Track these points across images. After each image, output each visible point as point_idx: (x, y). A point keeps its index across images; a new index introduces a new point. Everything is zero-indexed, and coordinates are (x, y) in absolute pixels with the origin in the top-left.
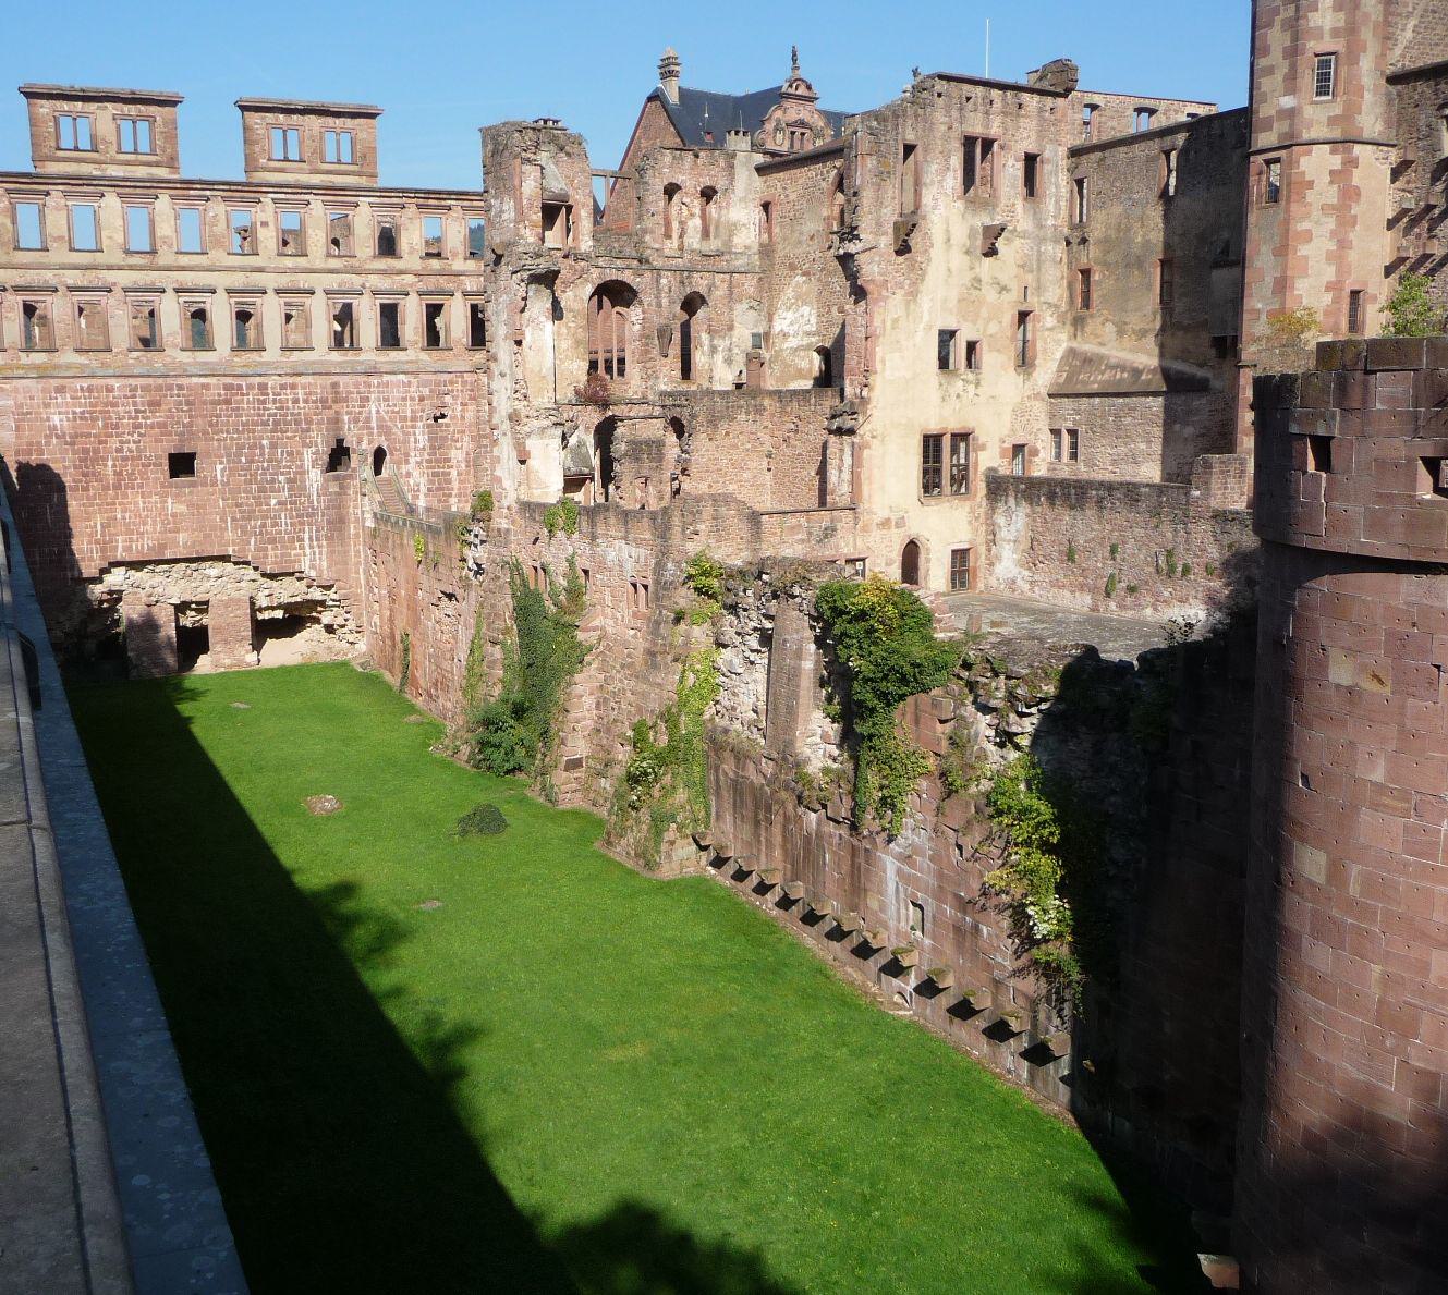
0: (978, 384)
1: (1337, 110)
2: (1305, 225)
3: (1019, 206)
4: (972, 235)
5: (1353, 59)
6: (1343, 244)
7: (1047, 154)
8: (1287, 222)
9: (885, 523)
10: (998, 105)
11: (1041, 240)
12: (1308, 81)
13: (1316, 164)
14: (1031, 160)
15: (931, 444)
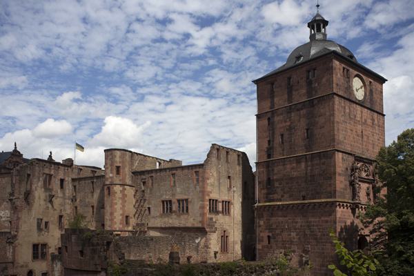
0: (48, 232)
1: (121, 178)
2: (115, 201)
3: (59, 191)
4: (46, 197)
5: (124, 168)
6: (124, 206)
7: (67, 179)
8: (112, 200)
9: (22, 266)
10: (53, 167)
11: (65, 199)
12: (115, 171)
13: (117, 189)
14: (62, 181)
15: (35, 246)
